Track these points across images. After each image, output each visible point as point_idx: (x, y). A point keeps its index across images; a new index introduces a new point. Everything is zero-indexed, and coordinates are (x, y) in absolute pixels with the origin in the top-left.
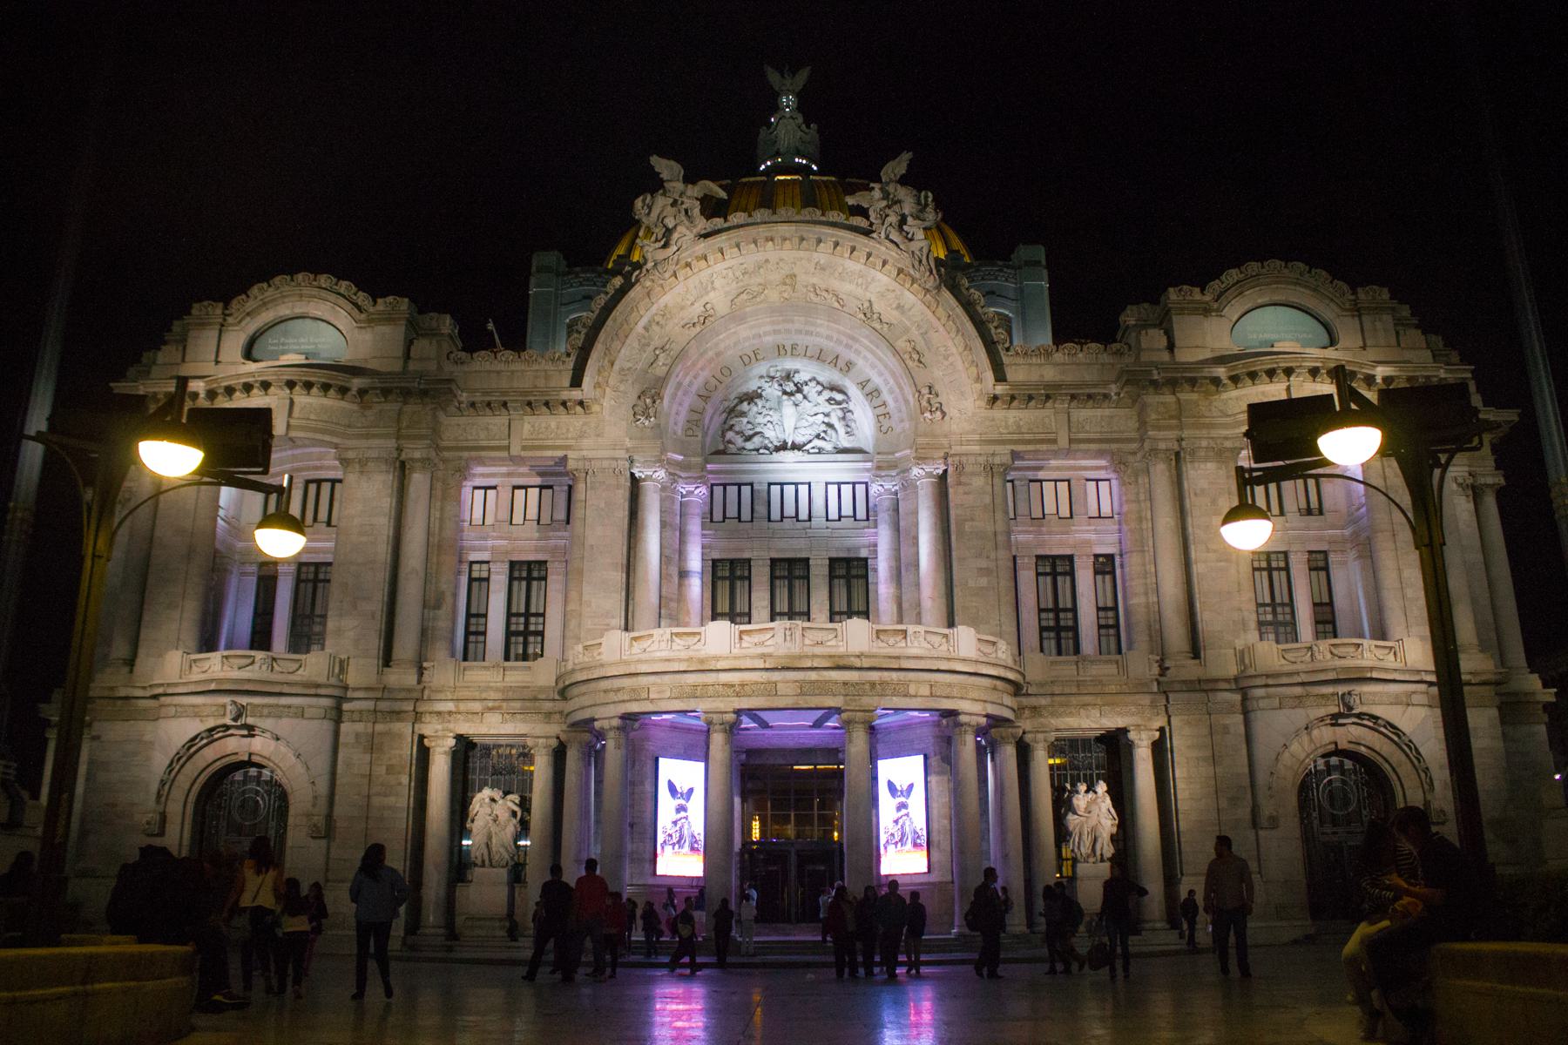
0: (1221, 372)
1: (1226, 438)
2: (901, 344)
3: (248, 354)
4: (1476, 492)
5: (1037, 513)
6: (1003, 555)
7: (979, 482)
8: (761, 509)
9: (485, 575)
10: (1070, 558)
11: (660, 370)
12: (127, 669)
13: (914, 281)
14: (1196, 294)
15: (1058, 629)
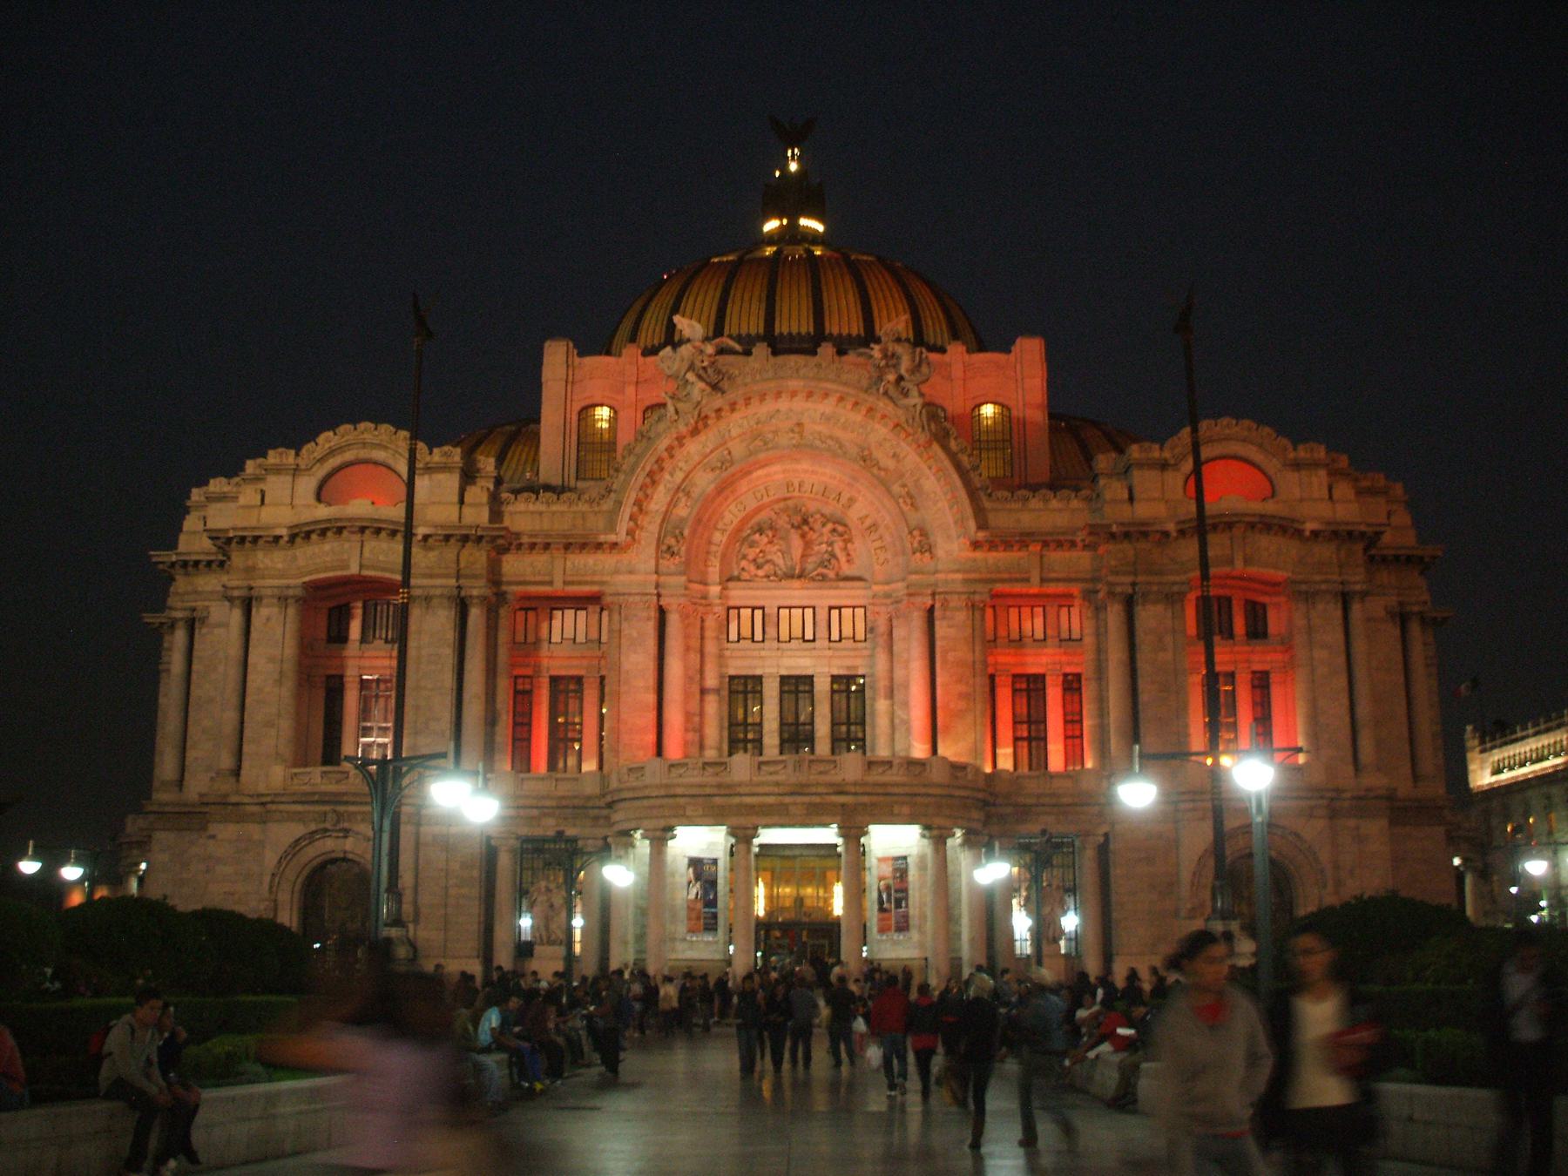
0: (1171, 527)
1: (1174, 583)
2: (896, 489)
3: (319, 498)
4: (1402, 618)
5: (1015, 635)
6: (981, 682)
7: (961, 616)
8: (771, 631)
9: (528, 687)
10: (1043, 676)
11: (682, 511)
12: (233, 780)
13: (908, 435)
14: (1156, 454)
15: (1029, 739)
